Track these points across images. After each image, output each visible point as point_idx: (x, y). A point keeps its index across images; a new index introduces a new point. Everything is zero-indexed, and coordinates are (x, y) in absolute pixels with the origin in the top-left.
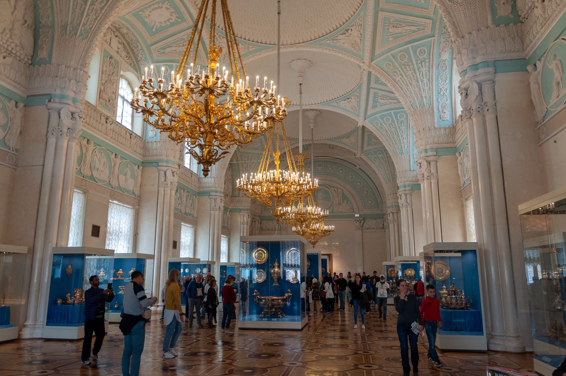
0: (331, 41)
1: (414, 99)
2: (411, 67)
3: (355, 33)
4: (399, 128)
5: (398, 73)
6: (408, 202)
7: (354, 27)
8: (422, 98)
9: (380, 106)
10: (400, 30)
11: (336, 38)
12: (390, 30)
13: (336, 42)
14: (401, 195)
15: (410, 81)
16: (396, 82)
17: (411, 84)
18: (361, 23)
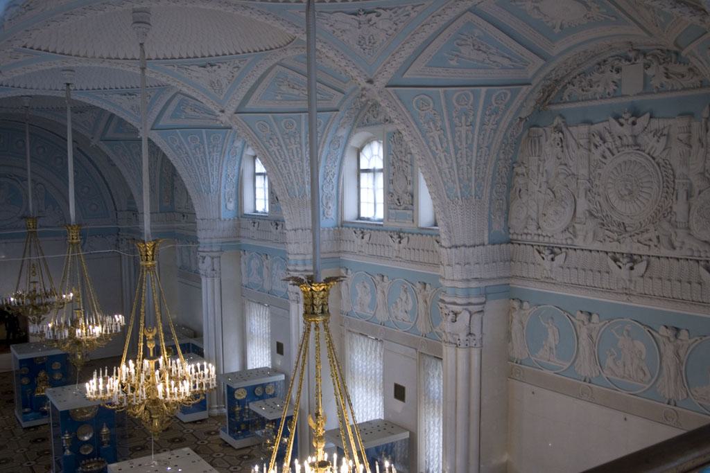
0: (176, 68)
1: (292, 183)
2: (298, 140)
3: (223, 72)
4: (209, 153)
5: (276, 141)
6: (216, 267)
7: (226, 65)
8: (304, 183)
9: (186, 118)
10: (296, 92)
11: (187, 67)
12: (282, 88)
13: (184, 71)
14: (204, 258)
15: (292, 157)
16: (268, 151)
17: (291, 161)
18: (240, 66)
